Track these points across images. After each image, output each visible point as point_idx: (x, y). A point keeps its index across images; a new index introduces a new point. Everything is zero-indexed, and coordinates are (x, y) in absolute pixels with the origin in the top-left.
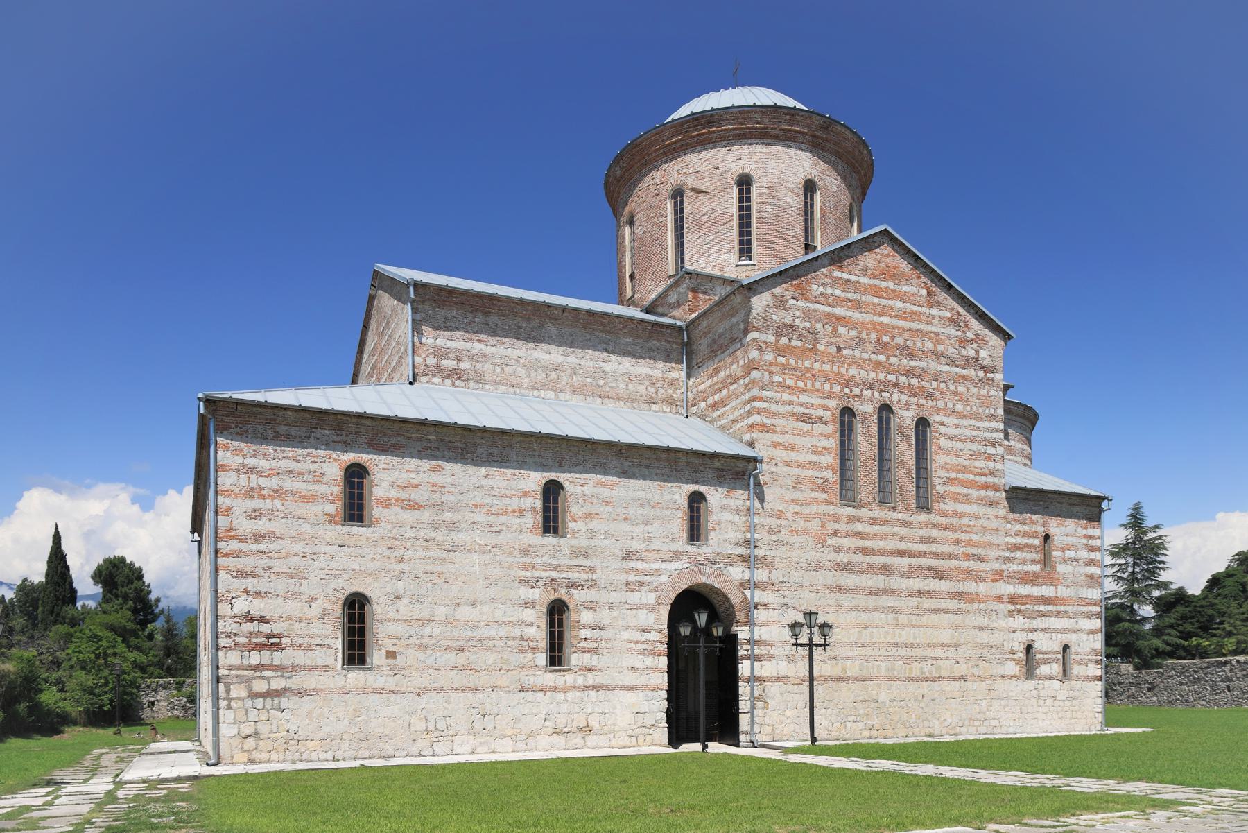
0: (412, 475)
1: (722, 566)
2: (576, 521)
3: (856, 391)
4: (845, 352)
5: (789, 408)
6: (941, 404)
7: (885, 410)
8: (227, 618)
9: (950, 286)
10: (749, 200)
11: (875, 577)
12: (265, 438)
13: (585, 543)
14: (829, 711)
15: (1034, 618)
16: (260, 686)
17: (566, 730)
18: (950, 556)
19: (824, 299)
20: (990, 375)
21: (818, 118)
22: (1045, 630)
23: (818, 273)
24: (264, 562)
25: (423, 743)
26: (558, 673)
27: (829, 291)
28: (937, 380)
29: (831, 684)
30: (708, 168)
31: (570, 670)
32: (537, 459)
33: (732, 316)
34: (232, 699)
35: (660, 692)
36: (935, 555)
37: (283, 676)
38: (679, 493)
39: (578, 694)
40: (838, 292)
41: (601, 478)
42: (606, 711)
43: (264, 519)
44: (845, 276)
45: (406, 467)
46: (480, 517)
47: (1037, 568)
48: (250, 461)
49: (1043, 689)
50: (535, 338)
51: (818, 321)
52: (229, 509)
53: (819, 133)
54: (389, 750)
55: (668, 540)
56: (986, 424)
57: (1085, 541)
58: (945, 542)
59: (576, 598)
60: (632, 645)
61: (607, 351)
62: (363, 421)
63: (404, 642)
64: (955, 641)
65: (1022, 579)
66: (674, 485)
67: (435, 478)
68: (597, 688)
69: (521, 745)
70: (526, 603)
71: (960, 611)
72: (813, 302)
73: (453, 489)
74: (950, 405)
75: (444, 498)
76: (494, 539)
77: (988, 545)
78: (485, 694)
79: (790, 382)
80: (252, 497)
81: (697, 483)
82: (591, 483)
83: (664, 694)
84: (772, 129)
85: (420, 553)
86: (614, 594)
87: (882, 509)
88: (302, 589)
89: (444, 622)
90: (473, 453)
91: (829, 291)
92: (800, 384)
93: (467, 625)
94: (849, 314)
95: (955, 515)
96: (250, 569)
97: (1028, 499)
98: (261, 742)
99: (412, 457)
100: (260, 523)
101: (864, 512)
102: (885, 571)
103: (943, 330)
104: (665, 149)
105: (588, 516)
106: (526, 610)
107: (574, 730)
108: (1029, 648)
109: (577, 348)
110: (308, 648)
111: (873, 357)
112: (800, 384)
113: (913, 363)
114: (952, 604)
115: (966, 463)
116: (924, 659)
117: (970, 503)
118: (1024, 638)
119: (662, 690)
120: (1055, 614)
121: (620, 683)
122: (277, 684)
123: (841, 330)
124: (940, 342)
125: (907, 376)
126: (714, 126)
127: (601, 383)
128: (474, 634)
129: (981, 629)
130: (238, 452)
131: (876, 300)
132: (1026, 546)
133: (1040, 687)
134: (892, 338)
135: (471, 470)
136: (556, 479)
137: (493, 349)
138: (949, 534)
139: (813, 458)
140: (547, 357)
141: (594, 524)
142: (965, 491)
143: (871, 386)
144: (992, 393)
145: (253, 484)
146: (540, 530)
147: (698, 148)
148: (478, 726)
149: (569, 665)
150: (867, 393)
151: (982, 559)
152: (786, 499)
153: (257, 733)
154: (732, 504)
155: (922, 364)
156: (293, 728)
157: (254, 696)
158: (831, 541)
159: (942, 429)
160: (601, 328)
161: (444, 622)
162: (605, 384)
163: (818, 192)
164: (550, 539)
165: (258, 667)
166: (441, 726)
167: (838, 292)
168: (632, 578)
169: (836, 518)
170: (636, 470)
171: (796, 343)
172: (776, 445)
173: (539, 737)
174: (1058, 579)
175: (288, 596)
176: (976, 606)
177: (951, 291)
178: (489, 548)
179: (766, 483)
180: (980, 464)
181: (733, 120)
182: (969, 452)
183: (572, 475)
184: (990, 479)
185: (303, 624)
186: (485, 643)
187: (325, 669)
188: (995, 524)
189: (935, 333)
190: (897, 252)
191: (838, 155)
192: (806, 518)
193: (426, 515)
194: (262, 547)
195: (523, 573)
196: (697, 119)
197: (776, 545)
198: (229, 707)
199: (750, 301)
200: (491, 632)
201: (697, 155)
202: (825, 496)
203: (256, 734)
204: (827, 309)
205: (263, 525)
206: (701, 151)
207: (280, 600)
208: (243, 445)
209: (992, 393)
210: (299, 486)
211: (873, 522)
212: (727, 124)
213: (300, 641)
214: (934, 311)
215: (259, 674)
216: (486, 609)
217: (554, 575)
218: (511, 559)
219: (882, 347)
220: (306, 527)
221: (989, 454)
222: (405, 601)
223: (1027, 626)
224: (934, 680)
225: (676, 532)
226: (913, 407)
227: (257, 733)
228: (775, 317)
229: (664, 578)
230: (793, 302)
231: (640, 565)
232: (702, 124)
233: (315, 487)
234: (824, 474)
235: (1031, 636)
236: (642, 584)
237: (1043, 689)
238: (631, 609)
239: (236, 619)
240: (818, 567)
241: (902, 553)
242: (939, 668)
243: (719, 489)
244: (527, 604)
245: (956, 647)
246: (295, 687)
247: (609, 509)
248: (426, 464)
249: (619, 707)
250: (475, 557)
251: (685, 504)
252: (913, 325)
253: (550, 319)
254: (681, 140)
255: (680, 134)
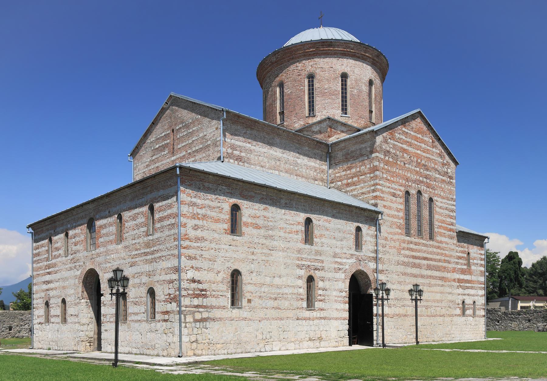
0: (257, 212)
1: (367, 262)
2: (317, 238)
3: (410, 184)
4: (407, 165)
5: (389, 189)
6: (436, 192)
7: (419, 192)
8: (185, 281)
9: (440, 139)
10: (346, 85)
11: (416, 269)
12: (200, 189)
13: (320, 249)
14: (402, 330)
15: (465, 289)
16: (198, 316)
17: (314, 339)
18: (440, 261)
19: (399, 140)
20: (451, 180)
21: (376, 51)
22: (468, 295)
23: (398, 128)
24: (199, 252)
25: (261, 345)
26: (311, 311)
27: (401, 137)
28: (435, 181)
29: (403, 318)
30: (327, 67)
31: (315, 310)
32: (303, 207)
33: (362, 143)
34: (187, 322)
35: (346, 320)
36: (435, 260)
37: (207, 311)
38: (351, 226)
39: (318, 321)
40: (404, 138)
41: (326, 218)
42: (328, 330)
43: (200, 230)
44: (406, 130)
45: (255, 207)
46: (282, 234)
47: (465, 267)
48: (194, 200)
49: (468, 320)
50: (271, 144)
51: (398, 150)
52: (185, 224)
53: (375, 58)
54: (249, 348)
55: (349, 249)
56: (450, 202)
57: (479, 256)
58: (438, 254)
59: (317, 275)
60: (336, 298)
61: (298, 153)
62: (240, 183)
63: (254, 295)
64: (441, 299)
65: (461, 272)
66: (351, 222)
67: (265, 213)
68: (324, 318)
69: (297, 346)
70: (299, 277)
71: (442, 286)
72: (396, 141)
73: (272, 219)
74: (439, 193)
75: (269, 224)
76: (288, 245)
77: (451, 256)
78: (284, 321)
79: (389, 178)
80: (194, 218)
81: (358, 222)
82: (322, 220)
83: (347, 322)
84: (357, 53)
85: (260, 251)
86: (330, 273)
87: (418, 238)
88: (215, 267)
89: (269, 285)
90: (279, 202)
91: (401, 137)
92: (392, 179)
93: (278, 287)
94: (407, 148)
95: (441, 242)
96: (194, 256)
97: (463, 236)
98: (198, 345)
99: (257, 203)
100: (198, 232)
101: (413, 239)
102: (419, 266)
103: (437, 159)
104: (305, 54)
105: (321, 236)
106: (299, 280)
107: (316, 338)
108: (463, 302)
109: (287, 150)
110: (217, 297)
112: (392, 179)
113: (428, 173)
114: (440, 282)
115: (444, 219)
116: (431, 307)
117: (446, 237)
118: (461, 298)
119: (347, 320)
120: (471, 287)
121: (332, 316)
122: (205, 315)
123: (405, 155)
124: (436, 164)
125: (426, 178)
126: (331, 47)
127: (296, 168)
128: (280, 291)
129: (450, 293)
130: (189, 195)
131: (416, 143)
132: (462, 257)
133: (467, 320)
134: (421, 160)
135: (279, 210)
136: (310, 217)
137: (254, 147)
138: (439, 251)
139: (396, 213)
140: (275, 153)
141: (323, 240)
142: (444, 232)
143: (415, 181)
144: (452, 188)
145: (195, 212)
146: (304, 241)
147: (323, 56)
148: (282, 337)
149: (314, 307)
150: (414, 185)
151: (449, 262)
152: (388, 232)
153: (197, 340)
154: (370, 233)
155: (431, 173)
156: (211, 338)
157: (196, 321)
158: (403, 252)
159: (437, 203)
160: (297, 142)
161: (269, 285)
162: (298, 169)
163: (374, 86)
164: (308, 246)
165: (197, 306)
166: (268, 337)
167: (404, 138)
168: (336, 266)
169: (404, 241)
170: (337, 215)
171: (391, 160)
172: (385, 206)
173: (304, 342)
174: (472, 272)
175: (209, 270)
176: (447, 283)
177: (440, 141)
178: (286, 249)
179: (381, 224)
180: (449, 220)
181: (341, 46)
182: (445, 214)
183: (315, 215)
184: (452, 227)
185: (215, 285)
186: (284, 296)
187: (224, 308)
188: (453, 247)
189: (435, 160)
190: (422, 122)
191: (380, 69)
192: (394, 241)
193: (262, 232)
194: (199, 244)
195: (298, 262)
196: (324, 42)
197: (385, 253)
198: (186, 327)
199: (375, 138)
200: (286, 291)
201: (322, 59)
202: (400, 231)
203: (196, 341)
204: (401, 145)
205: (199, 233)
206: (324, 58)
207: (206, 272)
208: (191, 191)
209: (452, 188)
210: (213, 214)
211: (416, 244)
212: (338, 48)
213: (214, 293)
214: (434, 150)
215: (197, 310)
216: (284, 279)
217: (309, 263)
218: (294, 255)
219: (418, 164)
220: (216, 235)
221: (451, 216)
222: (254, 274)
223: (463, 293)
224: (435, 316)
225: (352, 245)
226: (428, 193)
227: (197, 340)
228: (384, 147)
229: (347, 267)
230: (389, 140)
231: (339, 260)
232: (326, 45)
233: (219, 215)
234: (399, 221)
235: (464, 297)
236: (340, 269)
237: (468, 320)
238: (336, 281)
239: (188, 281)
240: (398, 264)
241: (425, 259)
242: (436, 311)
243: (366, 225)
244: (300, 277)
245: (442, 301)
246: (212, 317)
247: (328, 232)
248: (263, 206)
249: (332, 328)
250: (280, 253)
251: (354, 232)
252: (428, 155)
253: (277, 135)
254: (314, 51)
255: (314, 48)
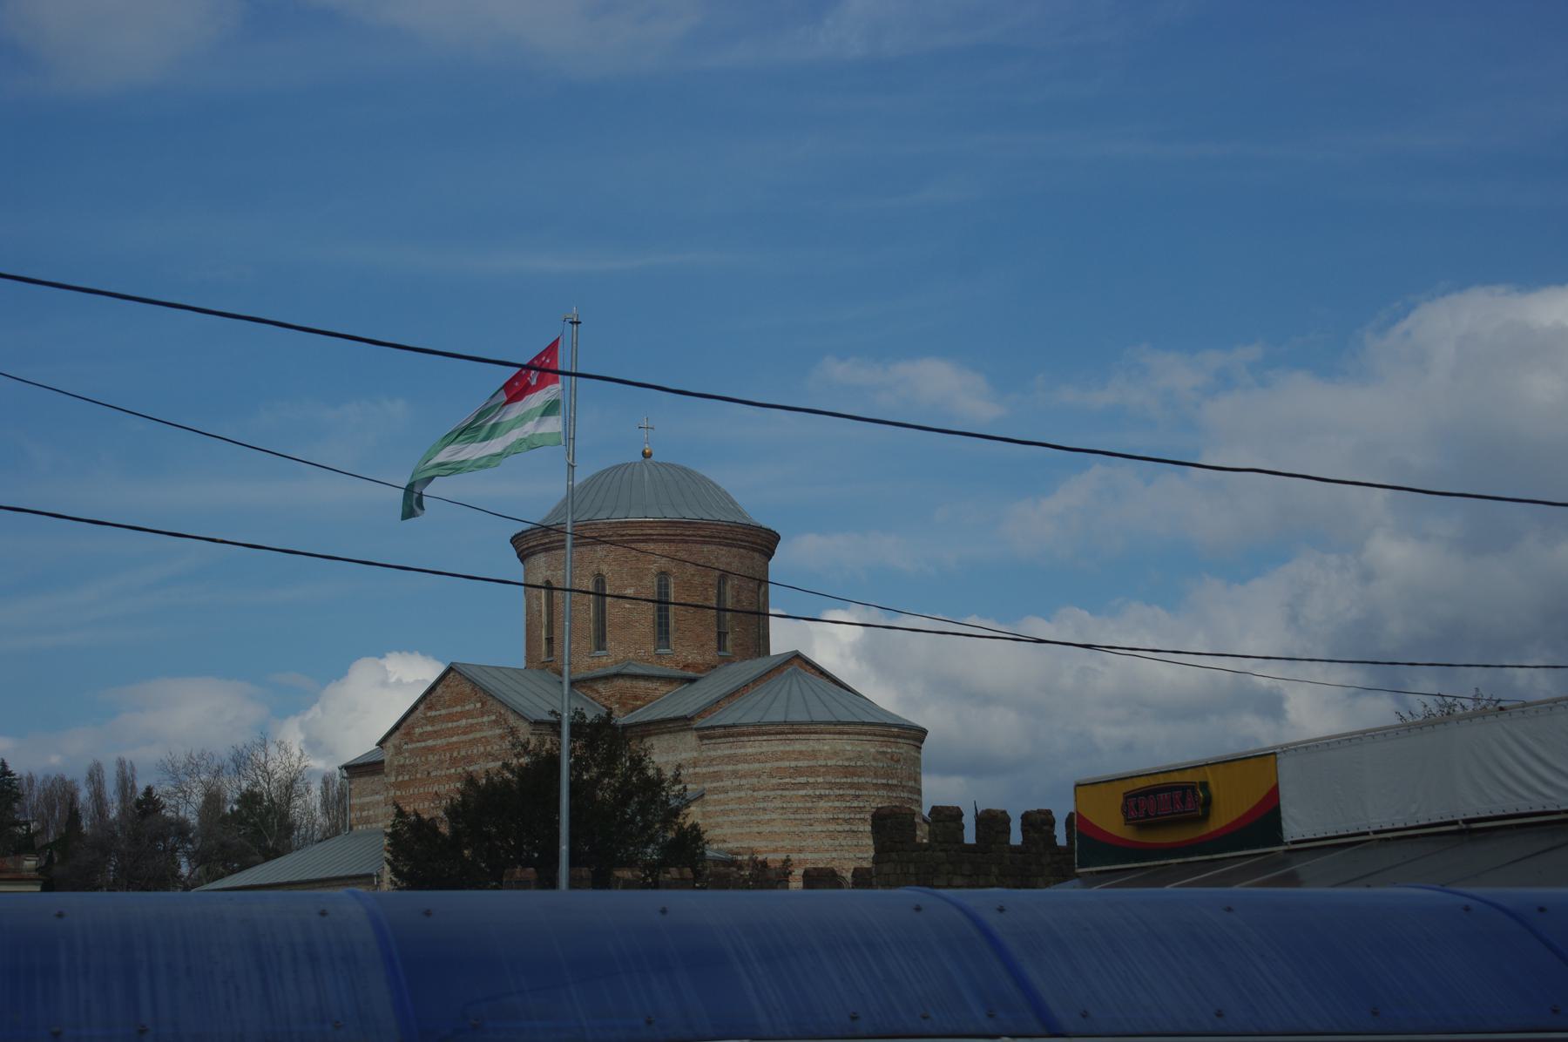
111: (448, 772)
123: (430, 757)
131: (450, 725)
167: (429, 728)
204: (423, 744)
214: (485, 719)
230: (405, 747)
